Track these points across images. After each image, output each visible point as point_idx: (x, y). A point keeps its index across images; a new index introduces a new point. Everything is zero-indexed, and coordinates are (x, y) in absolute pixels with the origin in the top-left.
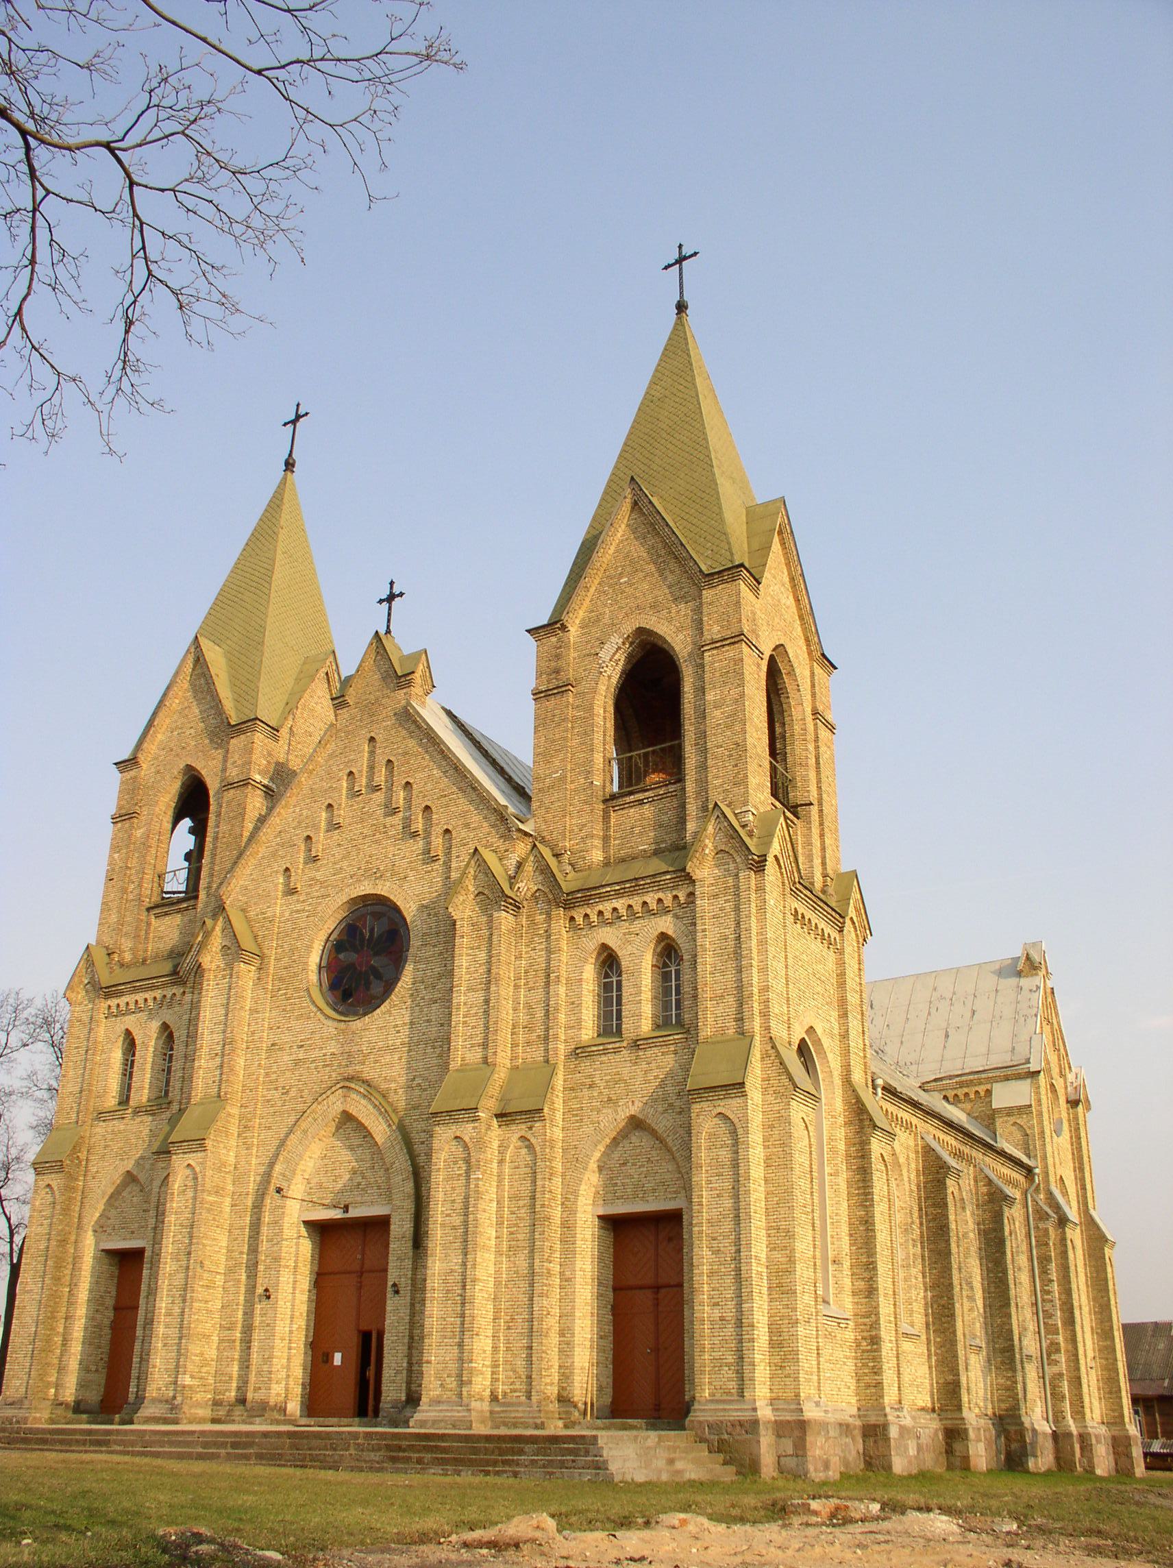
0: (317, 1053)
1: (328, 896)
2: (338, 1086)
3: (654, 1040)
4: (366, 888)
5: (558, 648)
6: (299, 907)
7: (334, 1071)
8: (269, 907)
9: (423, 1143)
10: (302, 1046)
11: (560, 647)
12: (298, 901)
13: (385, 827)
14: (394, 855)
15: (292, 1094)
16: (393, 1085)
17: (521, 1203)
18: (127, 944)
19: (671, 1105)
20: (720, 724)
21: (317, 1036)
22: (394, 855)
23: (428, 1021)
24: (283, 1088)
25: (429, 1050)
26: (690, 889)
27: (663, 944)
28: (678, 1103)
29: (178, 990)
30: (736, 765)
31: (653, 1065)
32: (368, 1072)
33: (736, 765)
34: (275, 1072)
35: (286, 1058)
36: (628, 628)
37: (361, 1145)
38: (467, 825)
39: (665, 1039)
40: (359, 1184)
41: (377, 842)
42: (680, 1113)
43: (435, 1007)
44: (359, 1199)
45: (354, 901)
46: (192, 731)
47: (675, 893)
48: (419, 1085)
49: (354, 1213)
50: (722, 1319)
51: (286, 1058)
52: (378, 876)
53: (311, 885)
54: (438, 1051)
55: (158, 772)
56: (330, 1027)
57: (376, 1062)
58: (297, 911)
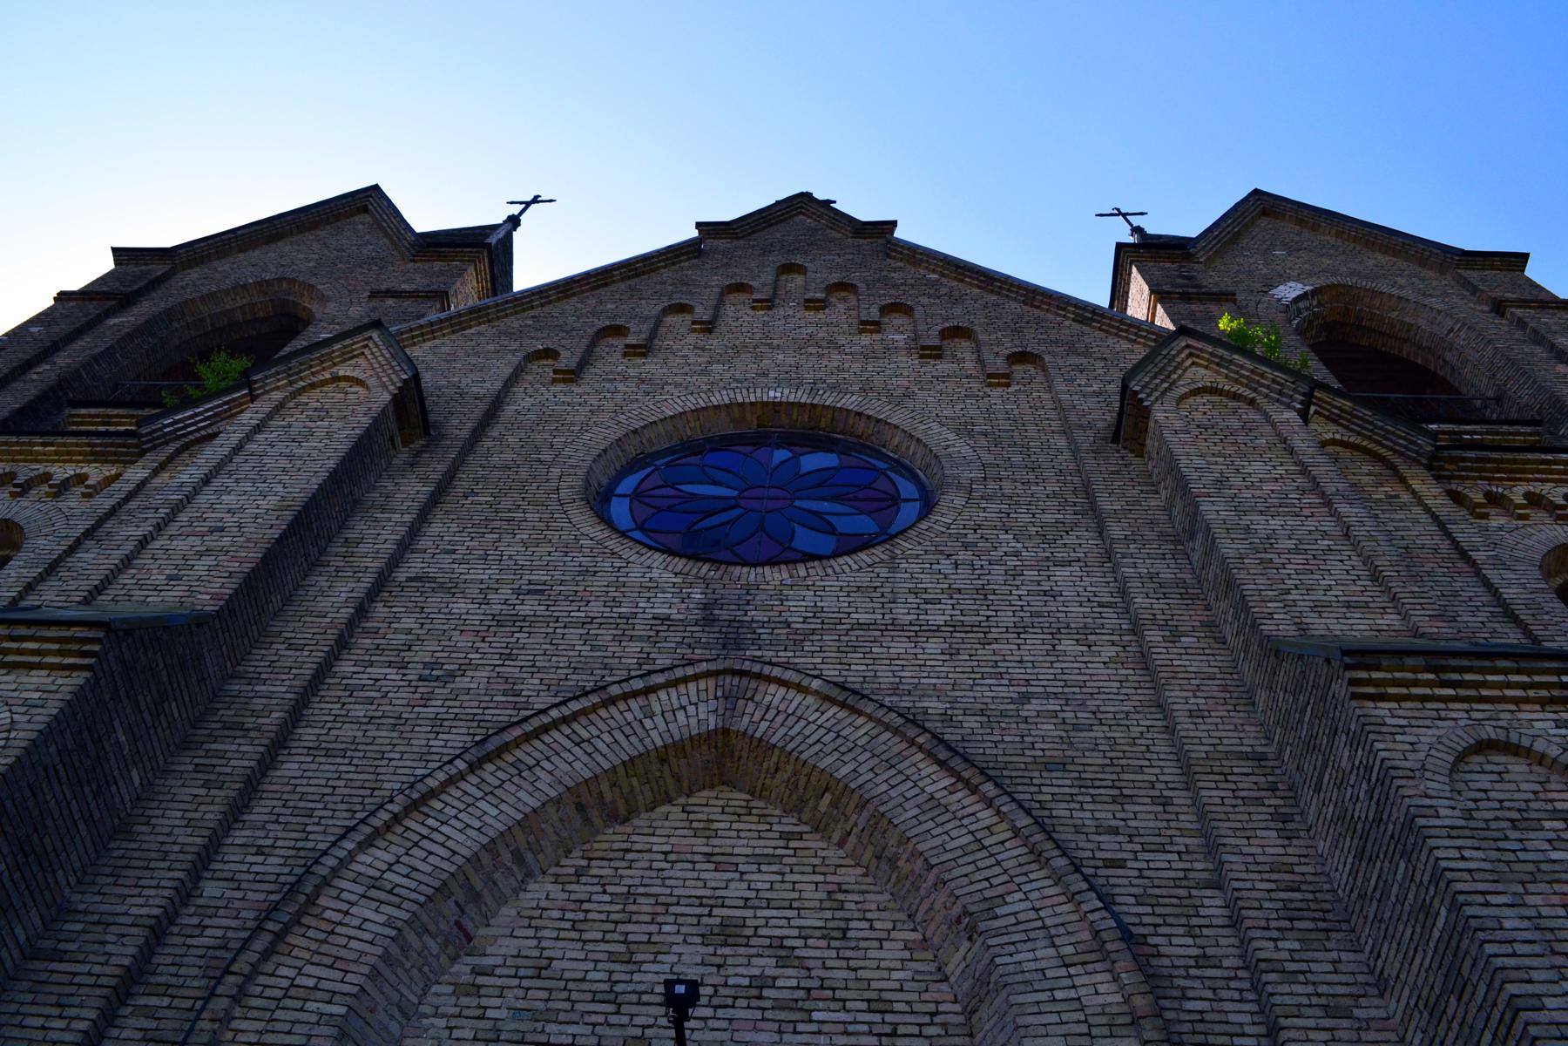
9: (1120, 864)
37: (759, 860)
40: (760, 984)
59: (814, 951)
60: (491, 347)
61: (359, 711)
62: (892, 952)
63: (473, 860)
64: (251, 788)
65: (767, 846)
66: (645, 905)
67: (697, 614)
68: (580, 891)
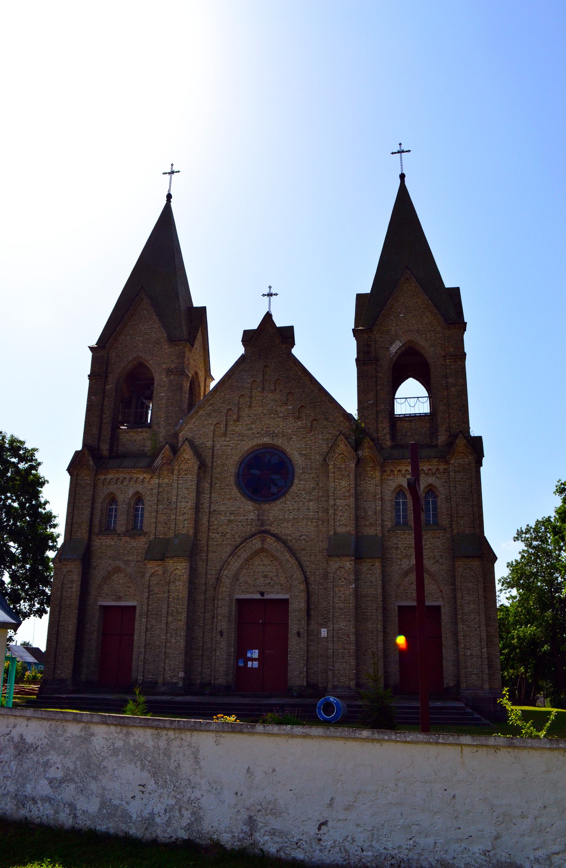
0: (242, 518)
1: (244, 441)
2: (259, 535)
3: (430, 531)
4: (266, 440)
5: (369, 341)
6: (225, 443)
7: (254, 527)
8: (208, 441)
9: (308, 566)
10: (233, 513)
11: (370, 341)
12: (225, 441)
13: (276, 411)
14: (283, 426)
15: (228, 536)
16: (289, 538)
17: (369, 599)
18: (105, 447)
19: (437, 561)
20: (455, 394)
21: (242, 510)
22: (283, 426)
23: (309, 509)
24: (222, 533)
25: (309, 523)
26: (446, 467)
27: (428, 488)
28: (441, 560)
29: (148, 476)
30: (464, 415)
31: (428, 542)
32: (274, 529)
33: (464, 415)
34: (216, 525)
35: (223, 518)
36: (404, 339)
37: (269, 565)
38: (327, 419)
39: (434, 531)
40: (269, 583)
41: (274, 418)
42: (442, 565)
43: (311, 503)
44: (270, 590)
45: (258, 445)
46: (140, 338)
47: (437, 467)
48: (304, 539)
49: (267, 597)
50: (471, 655)
51: (223, 518)
52: (274, 435)
53: (233, 434)
54: (314, 524)
55: (118, 356)
56: (249, 506)
57: (278, 525)
58: (225, 446)
59: (275, 578)
60: (206, 422)
61: (215, 543)
62: (283, 578)
63: (237, 572)
64: (207, 560)
65: (269, 563)
66: (256, 573)
67: (257, 518)
68: (249, 571)
